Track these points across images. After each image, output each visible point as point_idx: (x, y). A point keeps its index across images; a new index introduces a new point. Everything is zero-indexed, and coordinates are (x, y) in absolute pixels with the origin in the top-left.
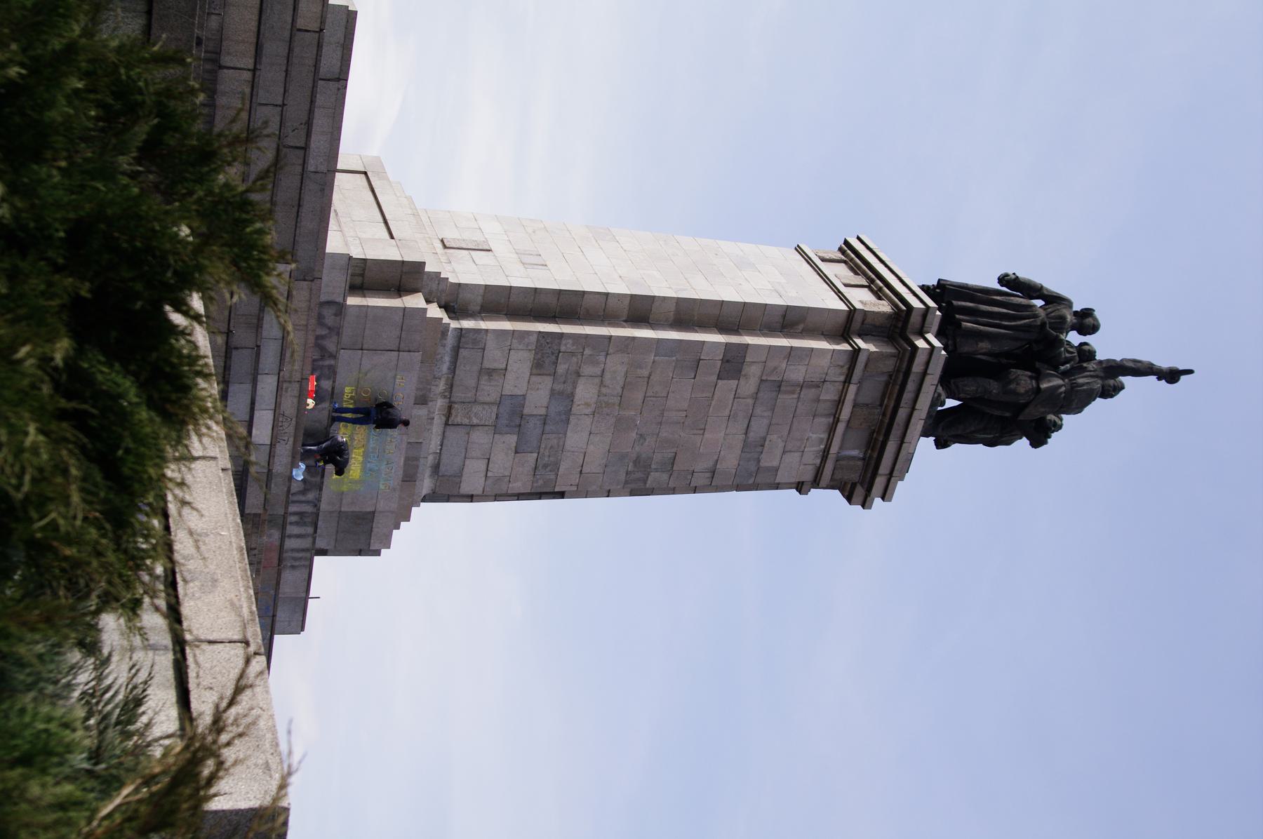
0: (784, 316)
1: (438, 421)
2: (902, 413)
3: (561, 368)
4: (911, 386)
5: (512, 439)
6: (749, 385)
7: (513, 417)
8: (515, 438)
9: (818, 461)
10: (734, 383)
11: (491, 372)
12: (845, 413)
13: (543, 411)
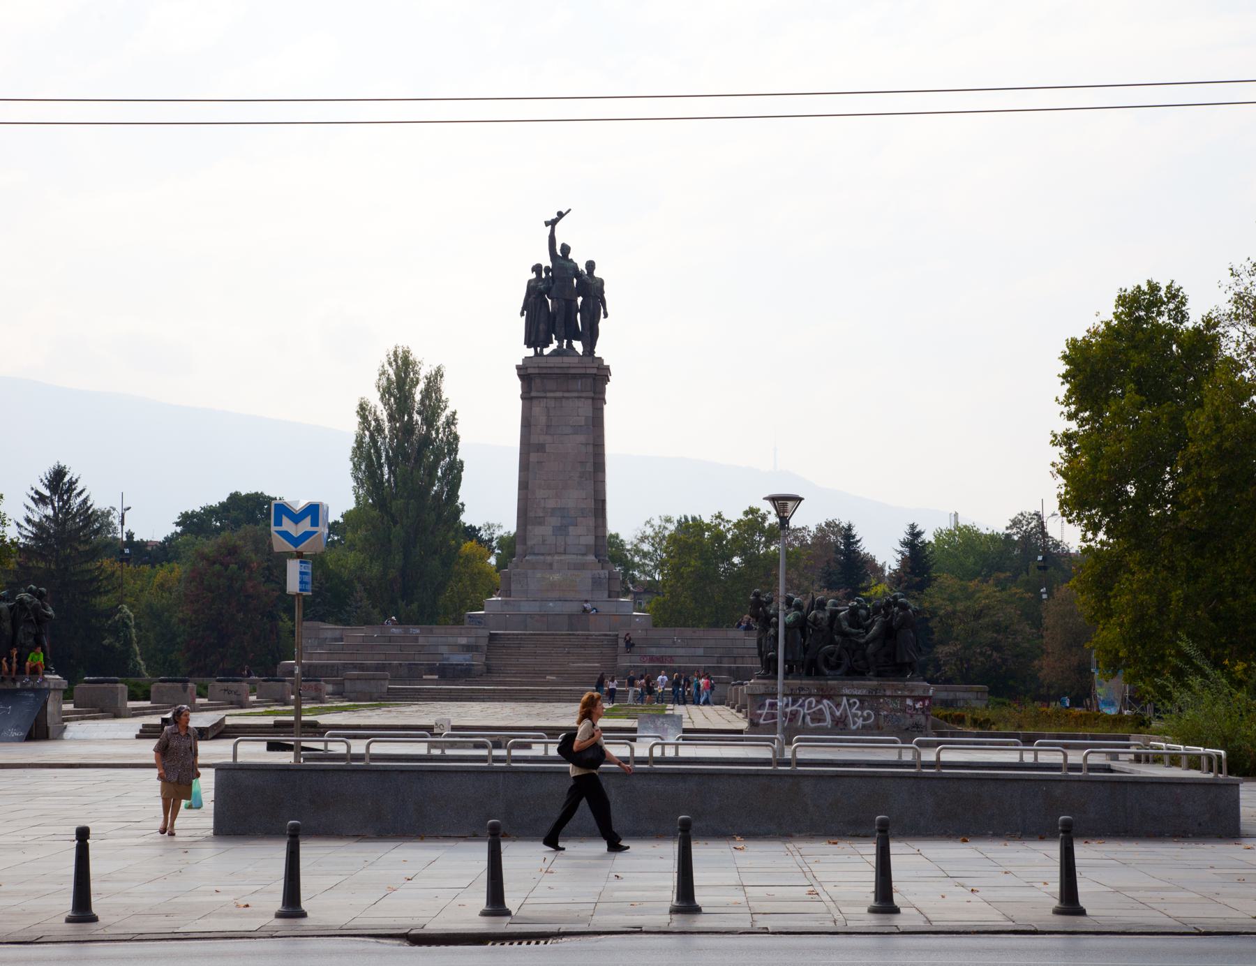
1: (563, 557)
2: (557, 371)
4: (545, 371)
5: (571, 528)
6: (549, 439)
7: (561, 530)
11: (544, 541)
12: (558, 394)
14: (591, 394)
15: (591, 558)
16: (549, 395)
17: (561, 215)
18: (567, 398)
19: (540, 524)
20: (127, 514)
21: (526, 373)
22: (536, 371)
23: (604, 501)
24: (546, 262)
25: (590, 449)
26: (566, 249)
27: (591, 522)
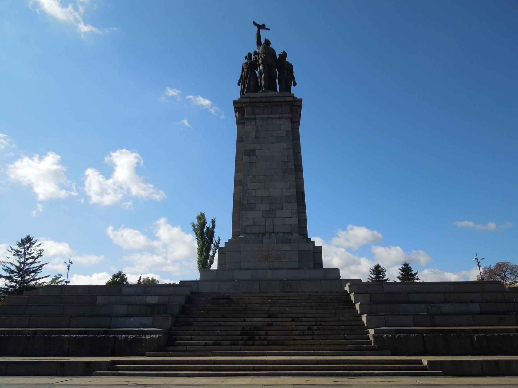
0: (240, 142)
2: (263, 100)
3: (253, 202)
4: (254, 100)
5: (278, 213)
8: (277, 211)
9: (284, 119)
10: (257, 151)
13: (268, 204)
14: (290, 115)
15: (296, 235)
16: (257, 116)
17: (263, 27)
18: (272, 119)
19: (252, 209)
20: (71, 265)
21: (239, 107)
22: (248, 100)
23: (303, 193)
24: (253, 48)
25: (291, 152)
26: (268, 43)
27: (295, 206)
